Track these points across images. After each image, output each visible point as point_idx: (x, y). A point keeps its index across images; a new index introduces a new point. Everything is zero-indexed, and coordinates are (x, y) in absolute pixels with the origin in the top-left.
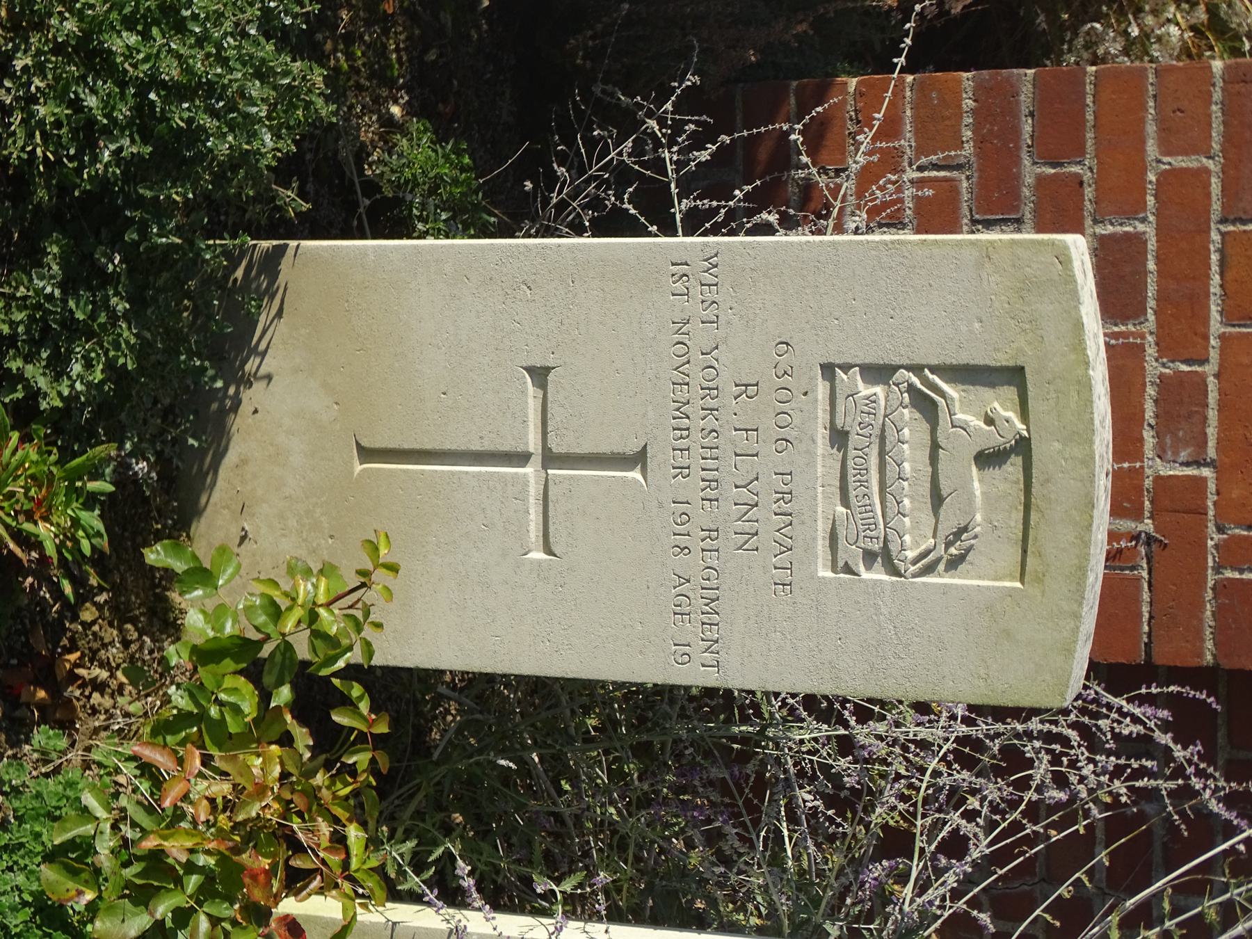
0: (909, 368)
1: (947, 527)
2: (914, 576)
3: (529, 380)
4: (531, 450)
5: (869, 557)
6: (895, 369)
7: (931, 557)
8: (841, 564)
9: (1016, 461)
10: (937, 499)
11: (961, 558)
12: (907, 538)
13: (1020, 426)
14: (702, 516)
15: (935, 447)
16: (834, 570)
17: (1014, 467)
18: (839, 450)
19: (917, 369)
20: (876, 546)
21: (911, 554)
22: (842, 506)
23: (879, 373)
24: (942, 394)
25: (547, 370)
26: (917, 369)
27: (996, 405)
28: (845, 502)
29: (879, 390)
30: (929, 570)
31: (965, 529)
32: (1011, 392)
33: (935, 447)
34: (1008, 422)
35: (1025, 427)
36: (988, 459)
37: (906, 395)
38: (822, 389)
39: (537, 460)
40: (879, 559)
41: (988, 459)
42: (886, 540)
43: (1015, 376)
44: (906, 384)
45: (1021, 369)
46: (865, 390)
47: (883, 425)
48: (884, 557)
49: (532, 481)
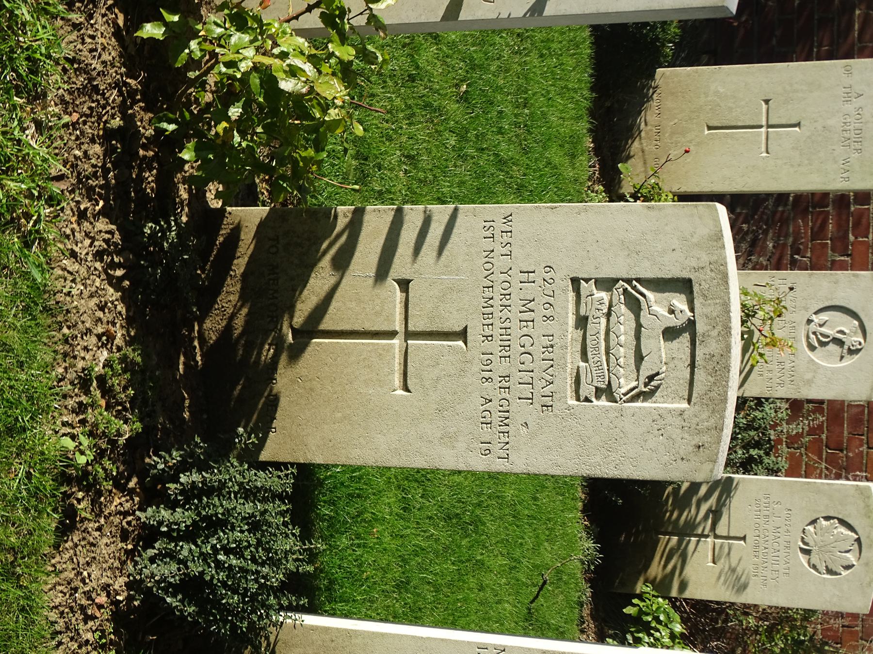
0: (623, 280)
1: (645, 372)
5: (599, 392)
6: (617, 280)
7: (636, 390)
8: (582, 398)
9: (687, 335)
10: (639, 358)
11: (652, 393)
12: (622, 380)
13: (690, 314)
14: (500, 367)
15: (639, 326)
16: (578, 399)
18: (581, 330)
19: (629, 281)
21: (623, 390)
22: (582, 361)
23: (607, 284)
25: (409, 281)
30: (633, 399)
31: (658, 374)
32: (683, 297)
33: (639, 326)
36: (670, 334)
37: (622, 297)
38: (571, 295)
41: (670, 334)
42: (609, 382)
43: (684, 286)
44: (621, 289)
48: (607, 392)
49: (397, 346)
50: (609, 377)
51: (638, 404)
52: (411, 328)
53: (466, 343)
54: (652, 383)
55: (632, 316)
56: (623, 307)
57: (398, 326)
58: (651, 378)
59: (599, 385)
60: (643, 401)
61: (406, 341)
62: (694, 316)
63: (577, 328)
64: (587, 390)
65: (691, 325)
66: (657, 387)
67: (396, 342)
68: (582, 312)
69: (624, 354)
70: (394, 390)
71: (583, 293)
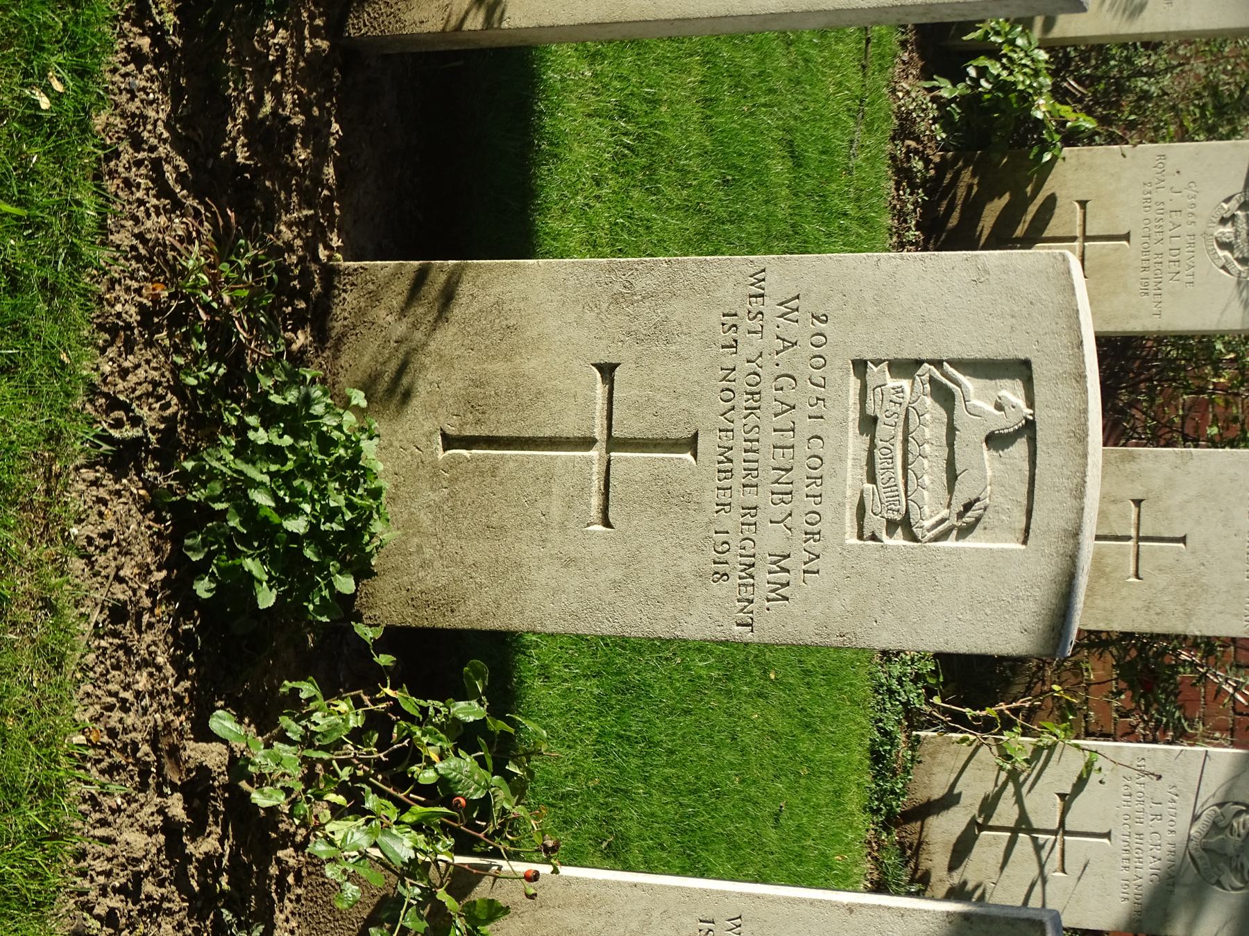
0: (931, 362)
1: (960, 498)
2: (930, 540)
3: (598, 375)
4: (598, 438)
5: (891, 526)
6: (919, 363)
7: (946, 524)
8: (867, 533)
10: (952, 476)
12: (926, 509)
15: (951, 430)
16: (860, 537)
17: (1020, 448)
19: (938, 364)
20: (898, 517)
21: (927, 524)
22: (868, 482)
23: (905, 367)
24: (959, 385)
26: (938, 364)
27: (1003, 393)
28: (872, 478)
29: (905, 383)
30: (944, 536)
31: (978, 500)
32: (1018, 385)
33: (951, 430)
34: (1014, 407)
35: (1031, 412)
36: (996, 441)
37: (928, 386)
38: (854, 383)
39: (601, 446)
40: (899, 530)
41: (996, 441)
43: (1021, 370)
44: (927, 375)
45: (1027, 364)
46: (891, 383)
47: (907, 410)
48: (904, 525)
50: (907, 505)
51: (951, 543)
52: (615, 433)
53: (695, 456)
54: (969, 514)
55: (943, 412)
56: (929, 401)
57: (599, 433)
58: (968, 507)
59: (891, 515)
60: (957, 539)
61: (608, 452)
62: (1033, 415)
63: (861, 434)
64: (875, 523)
65: (1029, 427)
66: (978, 520)
67: (594, 453)
68: (870, 411)
69: (930, 470)
70: (588, 525)
71: (871, 383)
